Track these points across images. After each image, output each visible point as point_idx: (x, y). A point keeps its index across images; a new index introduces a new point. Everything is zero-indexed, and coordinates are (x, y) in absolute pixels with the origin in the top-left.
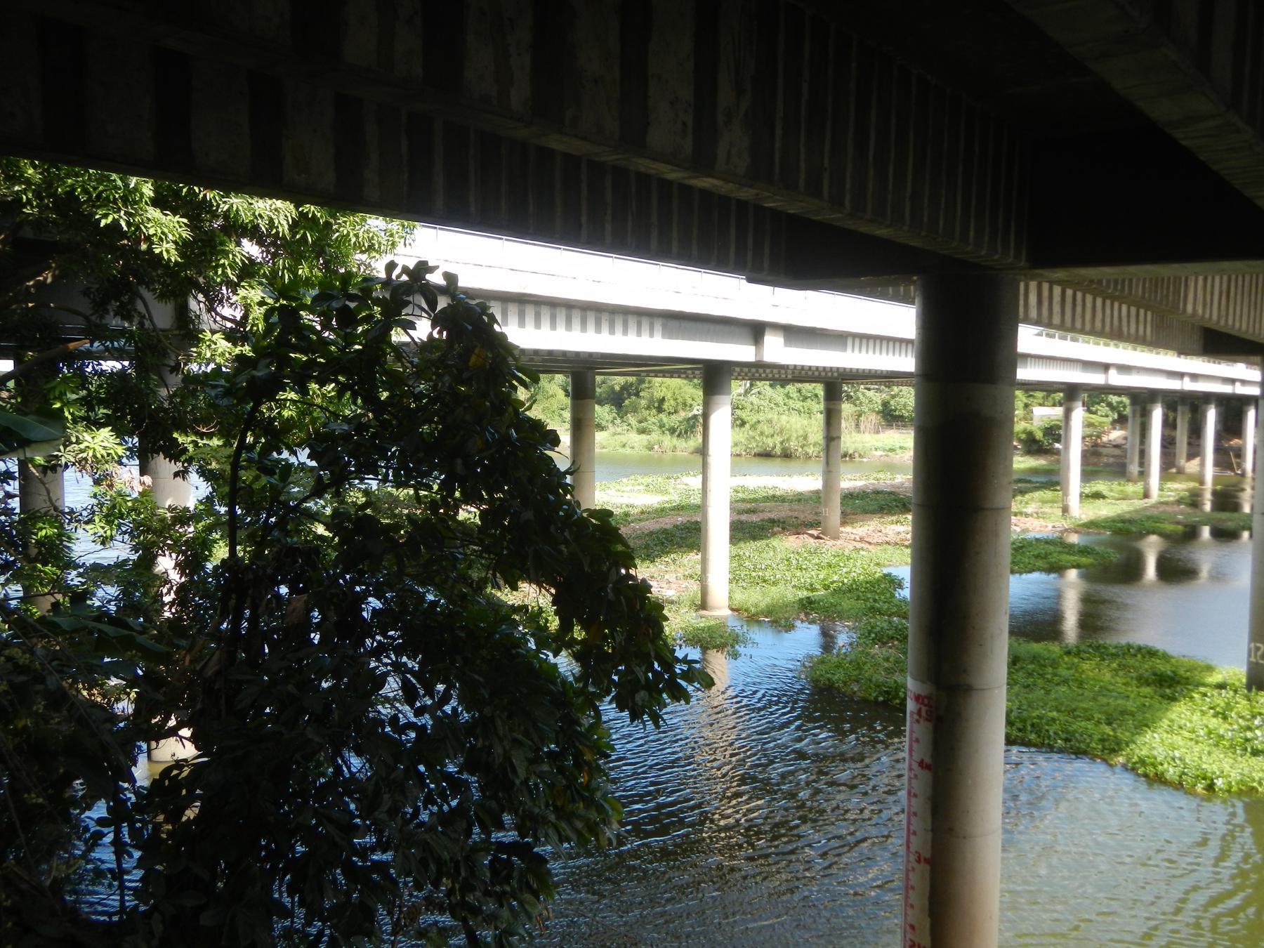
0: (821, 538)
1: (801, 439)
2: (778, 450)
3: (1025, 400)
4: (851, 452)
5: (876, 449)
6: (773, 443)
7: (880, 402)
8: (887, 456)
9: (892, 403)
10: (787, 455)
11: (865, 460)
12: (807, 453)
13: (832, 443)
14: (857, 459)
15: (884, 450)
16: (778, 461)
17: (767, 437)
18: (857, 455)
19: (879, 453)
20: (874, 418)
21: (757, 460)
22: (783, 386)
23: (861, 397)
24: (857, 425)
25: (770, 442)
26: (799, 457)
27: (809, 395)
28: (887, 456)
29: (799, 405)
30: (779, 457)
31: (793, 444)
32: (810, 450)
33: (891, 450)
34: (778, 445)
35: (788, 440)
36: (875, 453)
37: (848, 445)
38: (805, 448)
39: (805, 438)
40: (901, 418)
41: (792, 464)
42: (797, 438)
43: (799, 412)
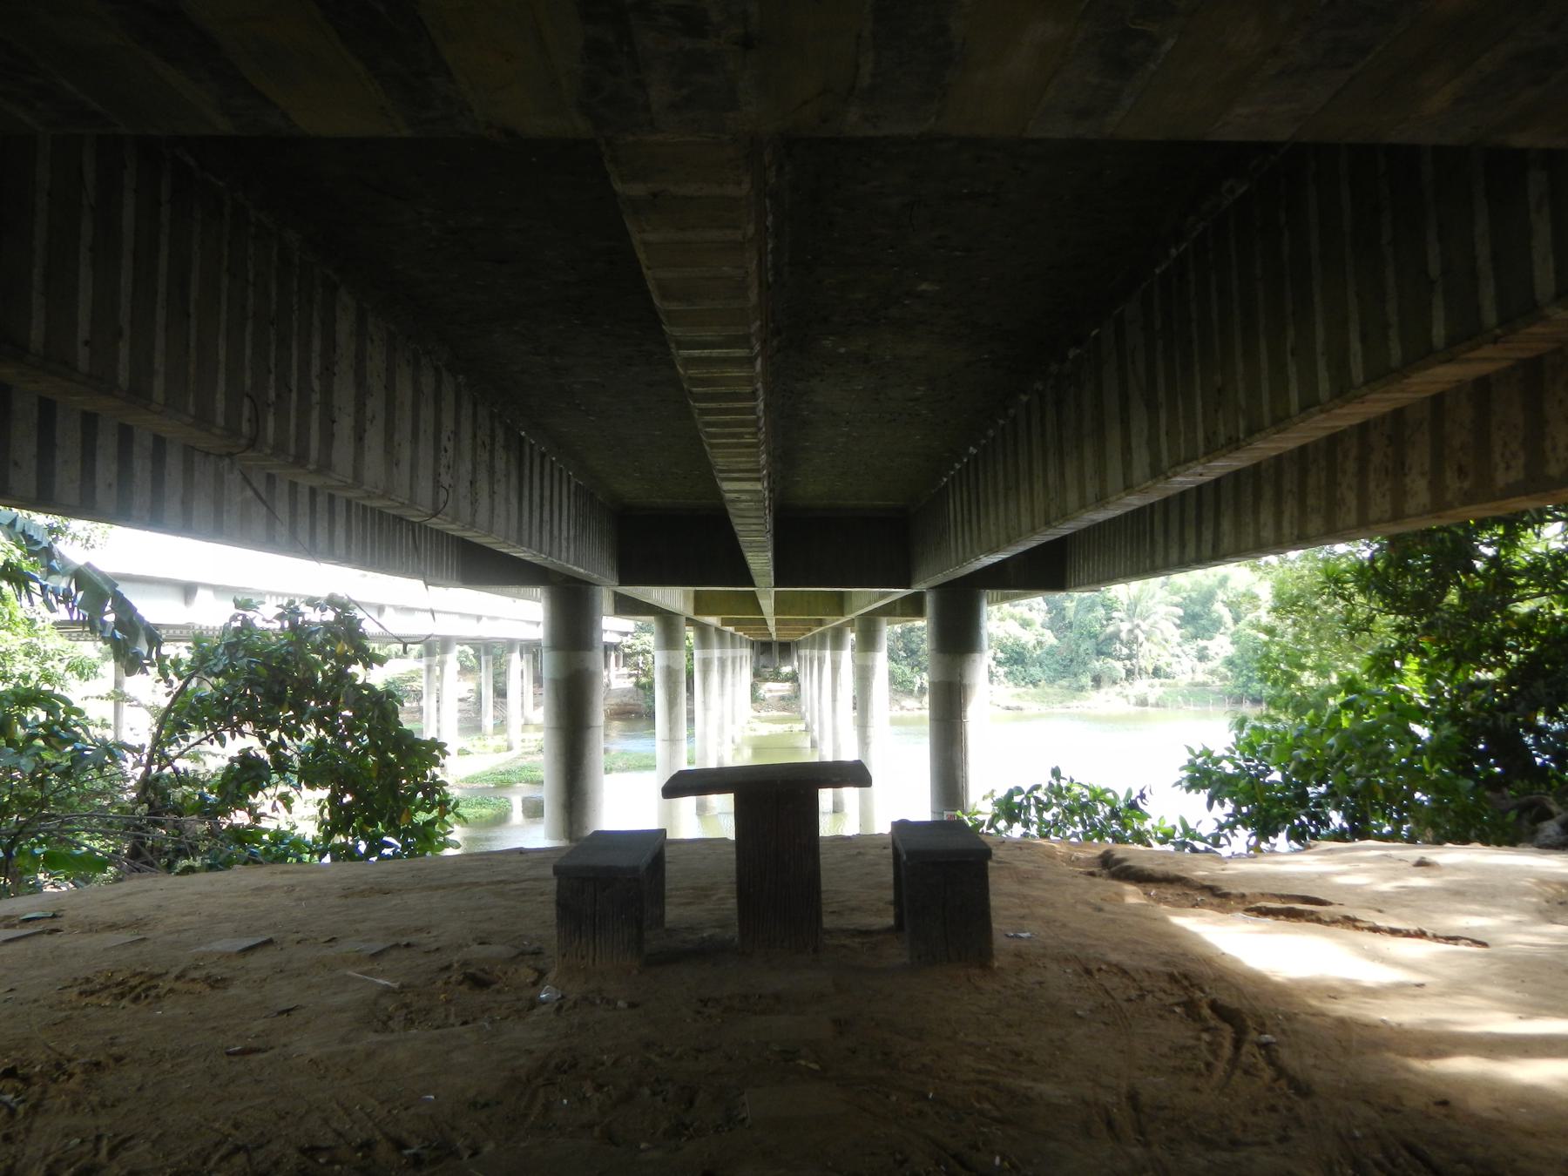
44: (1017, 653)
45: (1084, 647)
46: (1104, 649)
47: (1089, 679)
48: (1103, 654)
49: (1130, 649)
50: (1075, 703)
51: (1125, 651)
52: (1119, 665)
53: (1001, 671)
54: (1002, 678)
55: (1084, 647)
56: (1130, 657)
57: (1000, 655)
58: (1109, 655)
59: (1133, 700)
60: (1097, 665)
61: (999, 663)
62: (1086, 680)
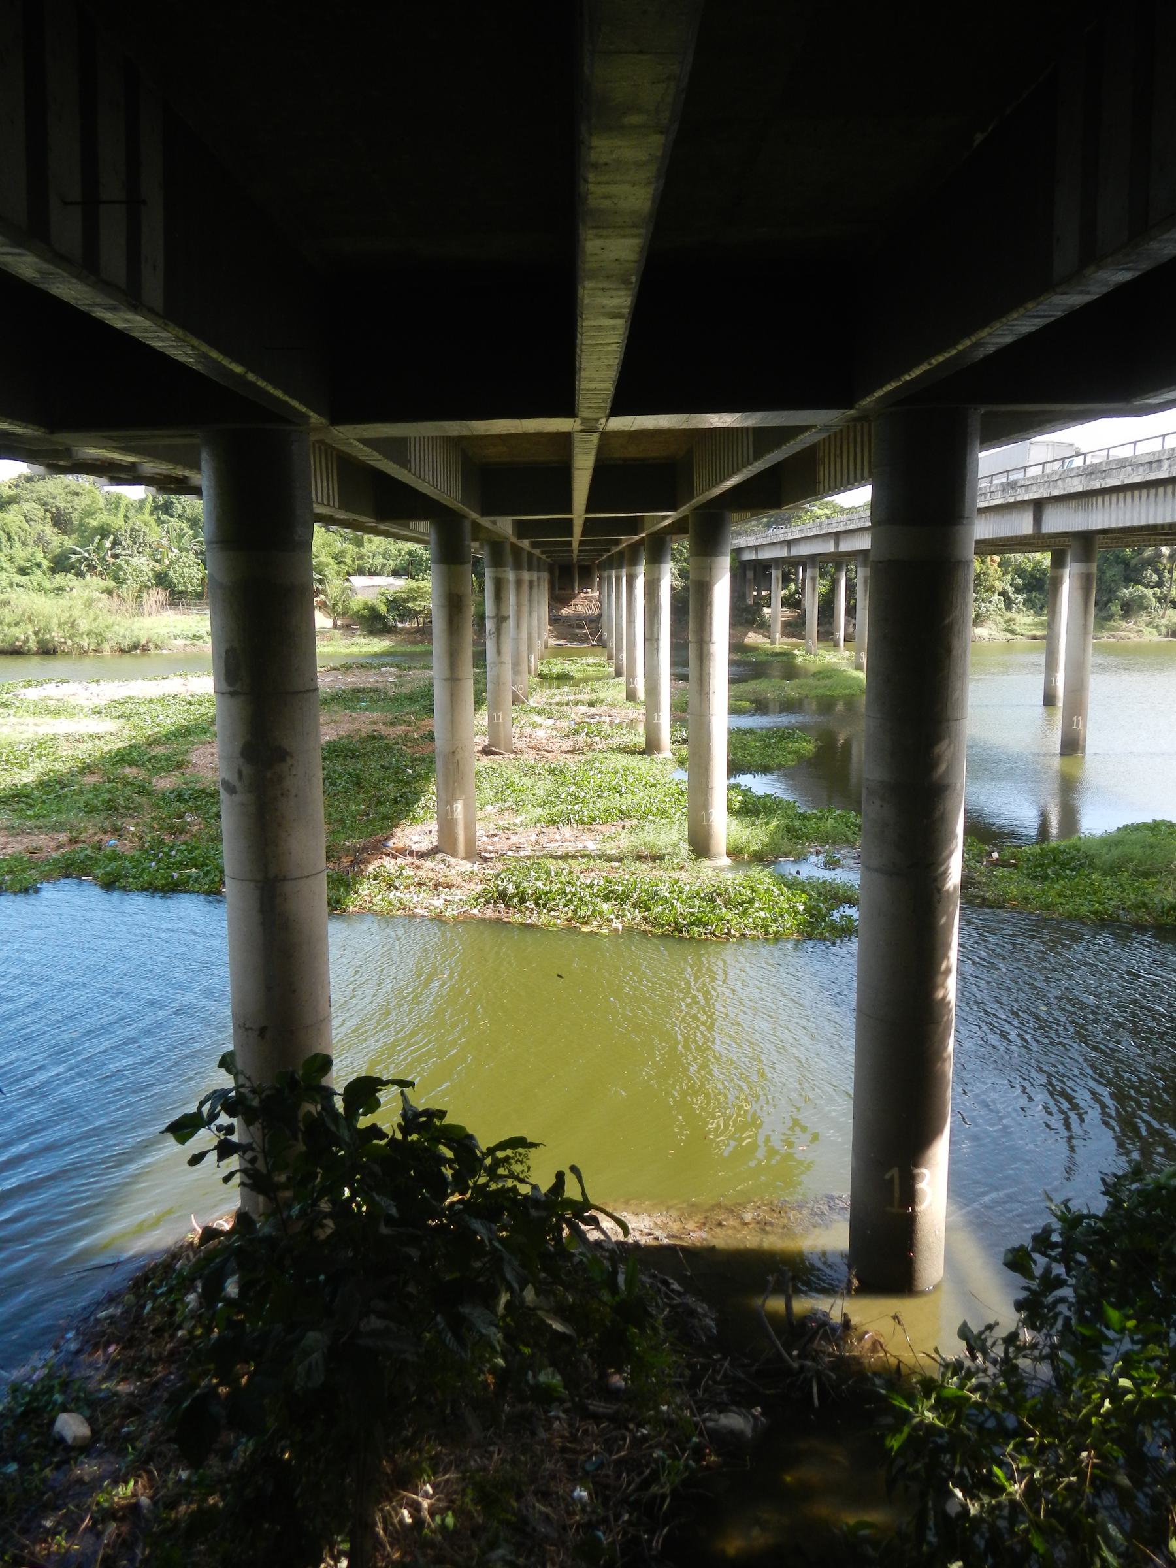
0: (495, 753)
1: (67, 627)
2: (33, 645)
3: (336, 567)
4: (143, 642)
5: (175, 637)
6: (23, 634)
7: (151, 574)
8: (194, 645)
9: (171, 573)
10: (47, 651)
11: (164, 652)
12: (80, 647)
13: (504, 625)
14: (153, 651)
15: (186, 638)
17: (9, 625)
18: (151, 646)
19: (180, 642)
20: (156, 596)
23: (125, 566)
24: (140, 605)
25: (17, 632)
26: (68, 653)
27: (27, 564)
28: (194, 645)
29: (23, 579)
30: (37, 653)
31: (56, 635)
32: (85, 643)
34: (33, 638)
35: (48, 630)
36: (174, 641)
37: (136, 633)
38: (75, 639)
39: (72, 625)
40: (184, 594)
41: (57, 666)
42: (60, 625)
44: (1036, 578)
45: (1109, 573)
46: (1133, 575)
47: (1119, 607)
48: (1131, 580)
49: (1160, 576)
50: (1105, 634)
51: (1155, 578)
52: (1149, 592)
53: (1020, 598)
54: (1021, 606)
55: (1109, 573)
56: (1159, 584)
57: (1019, 581)
58: (1138, 582)
59: (1164, 630)
60: (1126, 592)
61: (1018, 590)
62: (1115, 608)
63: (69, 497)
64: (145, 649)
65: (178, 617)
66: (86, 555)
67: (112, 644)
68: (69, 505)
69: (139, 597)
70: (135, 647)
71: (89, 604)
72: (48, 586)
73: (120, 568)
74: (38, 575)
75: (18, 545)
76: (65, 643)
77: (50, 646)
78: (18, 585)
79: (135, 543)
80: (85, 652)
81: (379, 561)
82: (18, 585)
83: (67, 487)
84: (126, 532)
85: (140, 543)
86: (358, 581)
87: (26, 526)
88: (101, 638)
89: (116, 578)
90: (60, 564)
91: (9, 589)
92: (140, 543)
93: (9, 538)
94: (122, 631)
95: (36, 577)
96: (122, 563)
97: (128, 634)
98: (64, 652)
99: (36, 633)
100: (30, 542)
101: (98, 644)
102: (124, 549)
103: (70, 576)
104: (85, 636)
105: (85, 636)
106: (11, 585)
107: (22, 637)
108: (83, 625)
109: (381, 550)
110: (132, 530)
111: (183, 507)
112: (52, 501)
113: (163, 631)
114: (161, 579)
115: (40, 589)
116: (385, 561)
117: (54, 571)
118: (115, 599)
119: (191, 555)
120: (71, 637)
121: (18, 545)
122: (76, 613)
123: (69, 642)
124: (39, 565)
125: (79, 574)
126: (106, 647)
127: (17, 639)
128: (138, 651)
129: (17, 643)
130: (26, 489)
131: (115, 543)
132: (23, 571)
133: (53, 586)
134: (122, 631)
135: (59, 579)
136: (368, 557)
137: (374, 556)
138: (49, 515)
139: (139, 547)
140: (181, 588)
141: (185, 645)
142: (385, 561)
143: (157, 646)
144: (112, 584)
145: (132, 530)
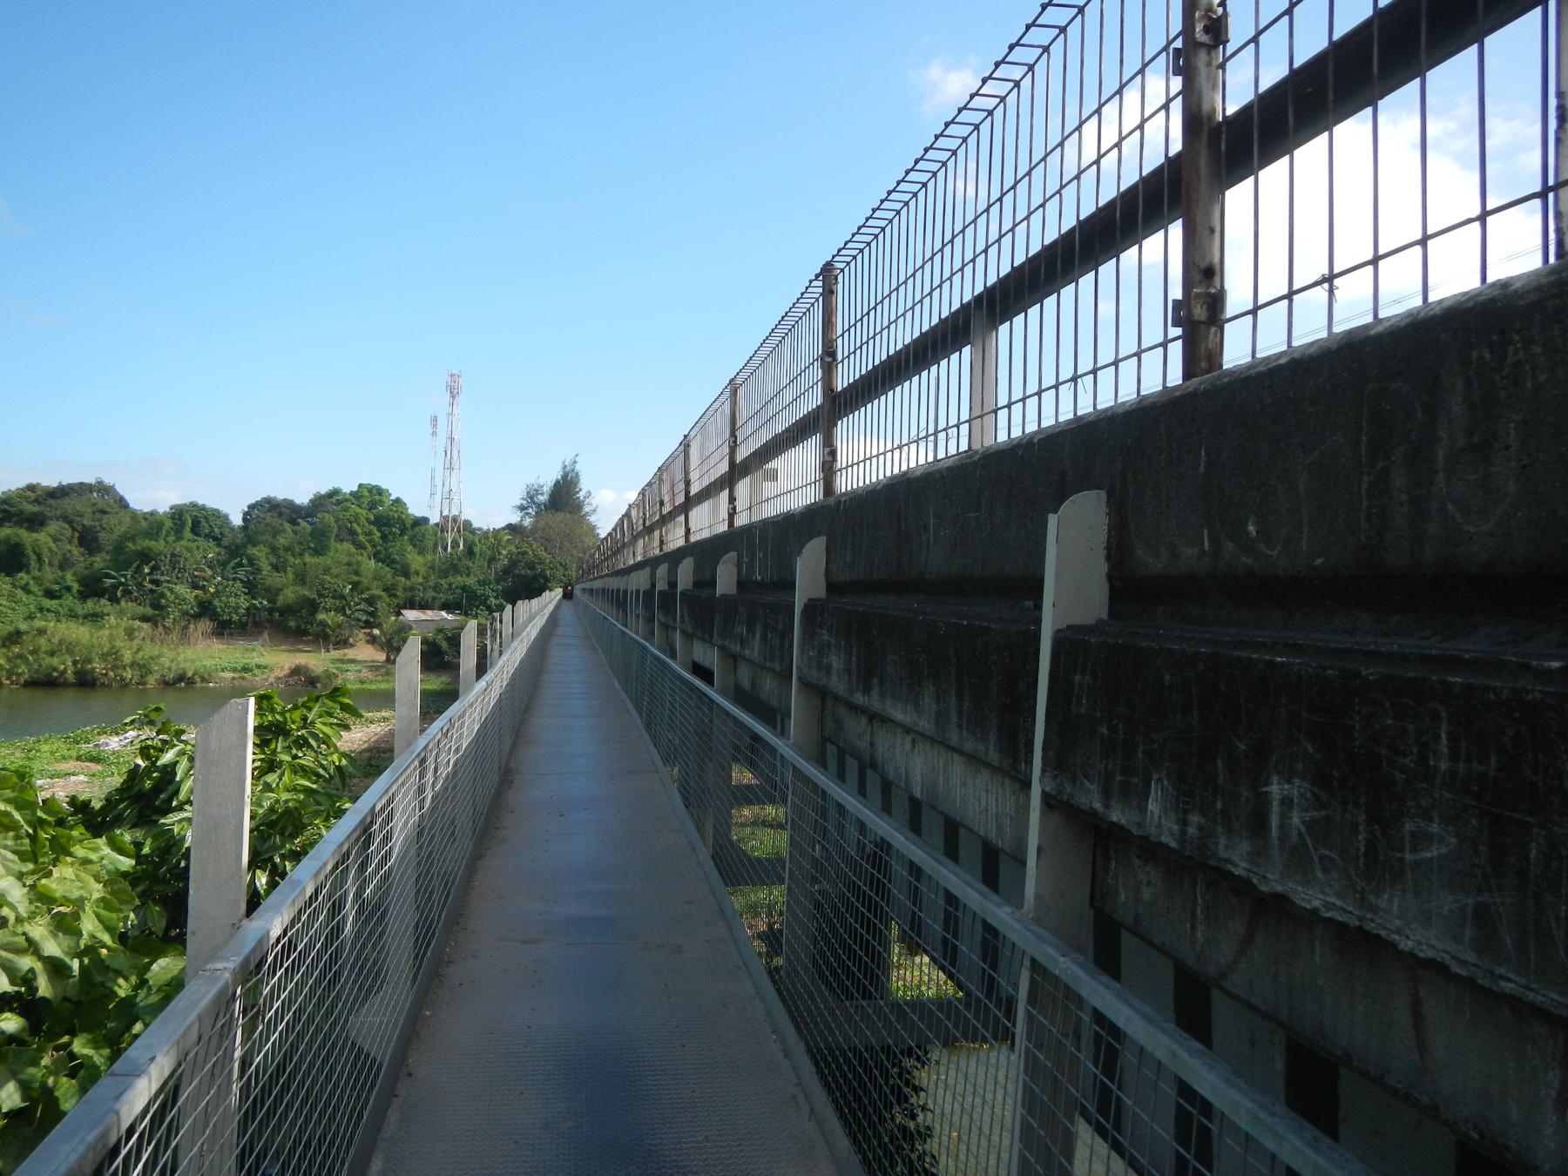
2: (70, 675)
4: (190, 674)
6: (65, 665)
8: (243, 678)
9: (216, 602)
10: (86, 682)
12: (123, 679)
15: (234, 670)
16: (71, 694)
18: (197, 679)
19: (228, 675)
21: (25, 694)
22: (8, 574)
26: (110, 686)
27: (56, 587)
30: (72, 685)
31: (98, 666)
32: (128, 674)
33: (246, 669)
36: (222, 674)
38: (120, 671)
43: (57, 613)
63: (98, 516)
64: (190, 682)
65: (221, 647)
66: (123, 580)
67: (156, 676)
68: (97, 523)
69: (186, 628)
70: (181, 678)
71: (130, 634)
72: (80, 610)
73: (163, 595)
74: (69, 601)
75: (47, 567)
76: (106, 674)
77: (89, 677)
78: (48, 610)
79: (174, 569)
80: (126, 685)
81: (430, 594)
82: (48, 610)
83: (94, 505)
84: (166, 557)
85: (180, 569)
86: (411, 615)
87: (53, 545)
88: (143, 668)
89: (156, 606)
90: (92, 588)
91: (39, 615)
92: (180, 569)
93: (40, 560)
94: (168, 664)
95: (68, 602)
96: (166, 591)
97: (174, 666)
98: (103, 683)
99: (75, 663)
100: (56, 563)
101: (142, 677)
102: (162, 574)
103: (104, 601)
104: (128, 669)
105: (128, 669)
106: (41, 610)
107: (62, 667)
108: (128, 657)
109: (431, 584)
110: (173, 555)
111: (211, 526)
112: (79, 519)
113: (209, 663)
114: (205, 609)
115: (72, 615)
116: (436, 595)
117: (83, 596)
118: (161, 629)
119: (238, 584)
120: (114, 668)
121: (47, 567)
122: (118, 643)
123: (111, 674)
124: (69, 589)
125: (114, 600)
126: (152, 681)
127: (55, 669)
128: (183, 684)
129: (55, 674)
130: (51, 506)
131: (154, 569)
132: (50, 594)
133: (85, 611)
134: (168, 664)
135: (90, 605)
136: (419, 590)
137: (425, 589)
138: (77, 534)
139: (179, 572)
140: (226, 617)
141: (234, 678)
142: (436, 595)
143: (203, 679)
144: (149, 611)
145: (173, 555)
